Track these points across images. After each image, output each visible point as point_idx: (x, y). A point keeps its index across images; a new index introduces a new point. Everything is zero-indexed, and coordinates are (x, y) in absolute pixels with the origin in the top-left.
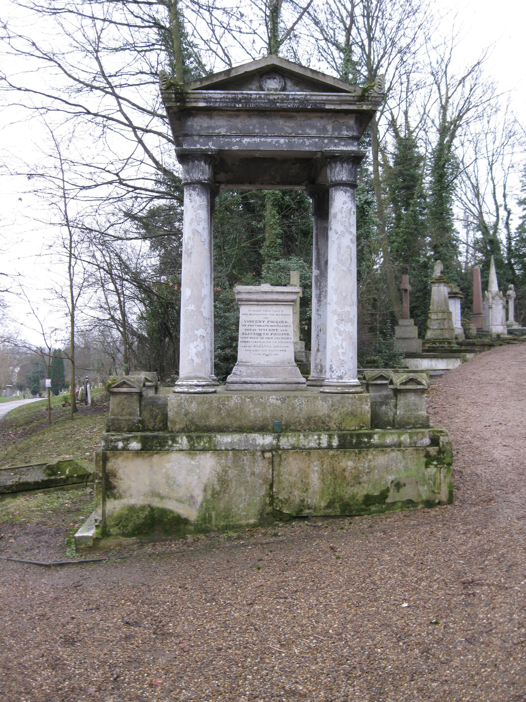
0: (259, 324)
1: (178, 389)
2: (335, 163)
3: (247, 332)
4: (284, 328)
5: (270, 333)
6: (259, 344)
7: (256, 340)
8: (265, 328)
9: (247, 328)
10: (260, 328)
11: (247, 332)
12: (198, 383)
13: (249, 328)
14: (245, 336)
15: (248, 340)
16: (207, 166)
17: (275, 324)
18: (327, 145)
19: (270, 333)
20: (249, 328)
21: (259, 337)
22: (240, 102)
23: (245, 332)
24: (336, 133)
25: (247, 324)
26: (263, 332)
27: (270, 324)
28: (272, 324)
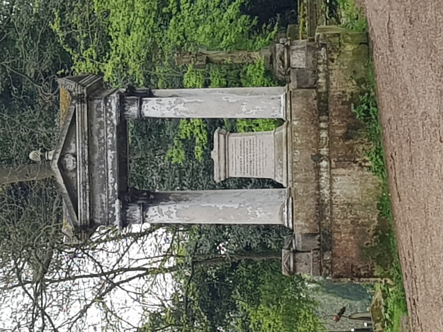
1: (291, 225)
2: (125, 115)
12: (286, 211)
16: (130, 207)
18: (112, 121)
24: (102, 115)
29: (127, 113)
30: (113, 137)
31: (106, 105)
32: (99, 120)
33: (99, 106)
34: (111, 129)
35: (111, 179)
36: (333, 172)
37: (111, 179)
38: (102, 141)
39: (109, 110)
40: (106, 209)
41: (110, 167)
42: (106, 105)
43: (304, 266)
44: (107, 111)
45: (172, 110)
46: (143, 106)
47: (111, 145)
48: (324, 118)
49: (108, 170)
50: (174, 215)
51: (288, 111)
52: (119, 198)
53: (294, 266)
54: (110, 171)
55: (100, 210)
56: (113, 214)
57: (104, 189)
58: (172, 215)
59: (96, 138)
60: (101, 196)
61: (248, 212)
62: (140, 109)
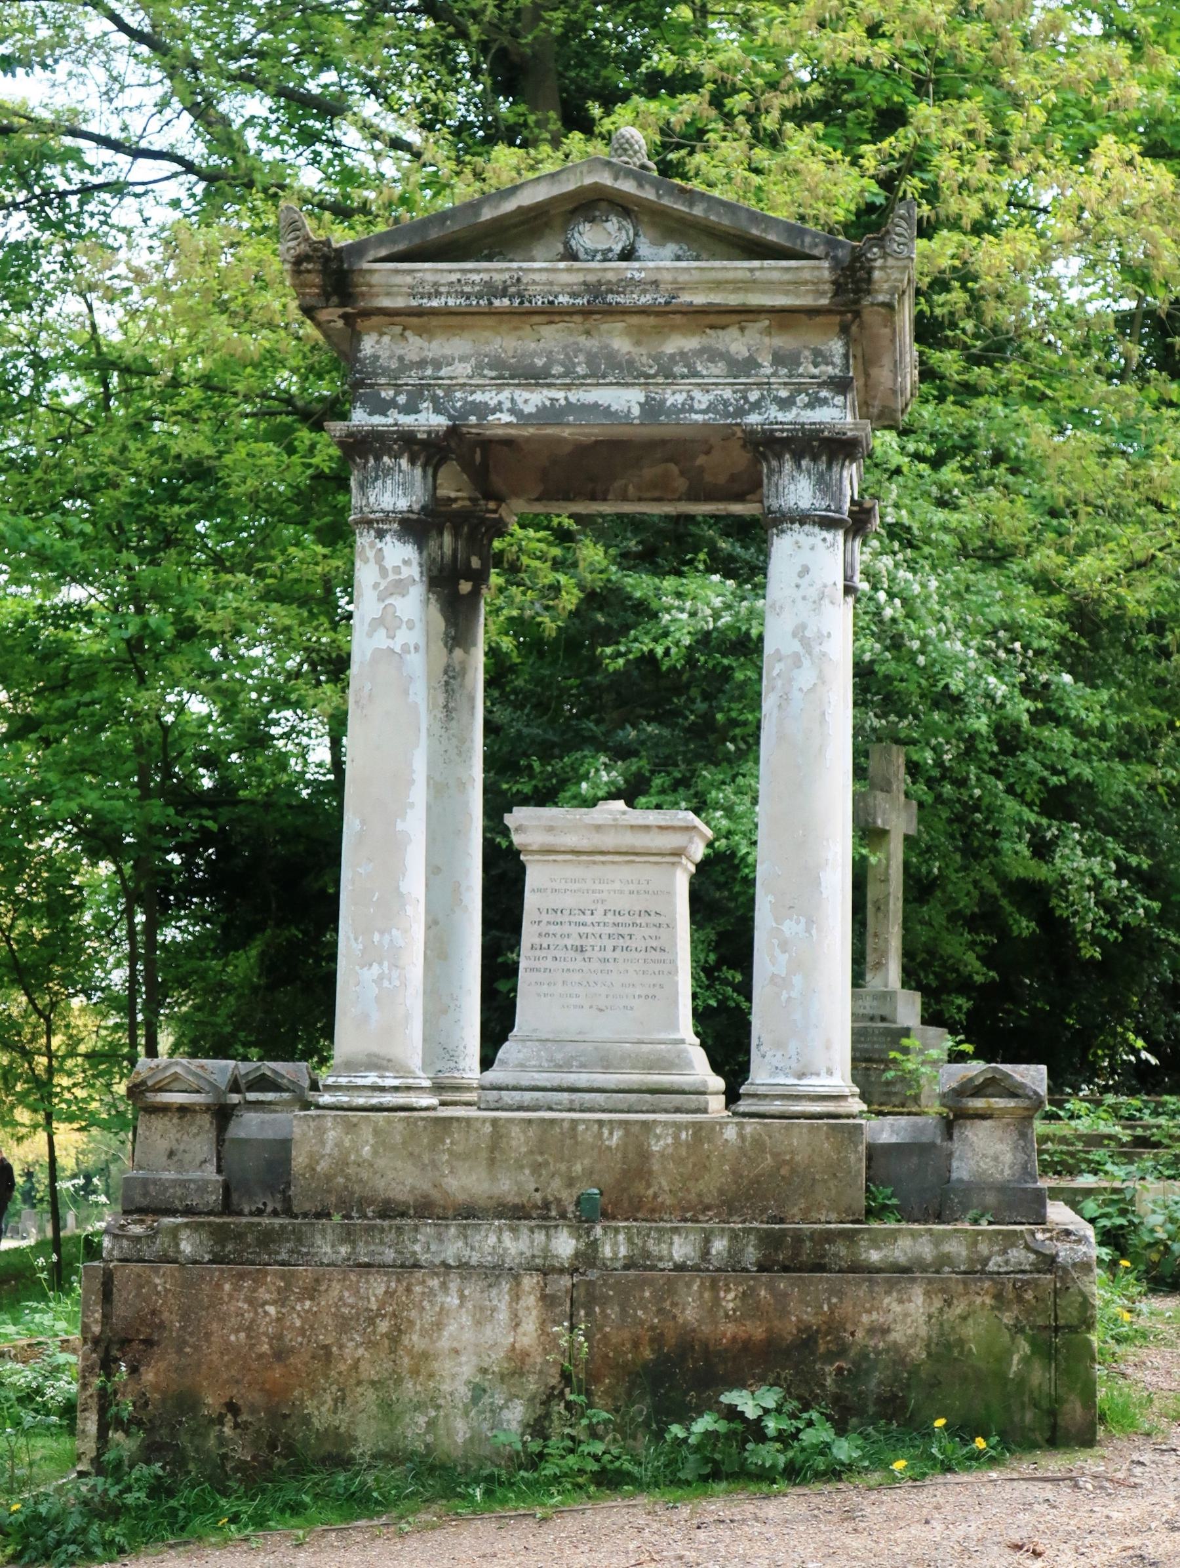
0: (582, 918)
2: (779, 457)
3: (545, 942)
4: (652, 931)
5: (610, 944)
6: (576, 977)
7: (571, 966)
8: (597, 930)
9: (544, 928)
10: (582, 930)
11: (545, 942)
12: (380, 1082)
13: (552, 929)
14: (538, 953)
15: (549, 963)
16: (418, 471)
17: (626, 919)
18: (756, 406)
19: (610, 944)
20: (552, 929)
21: (579, 956)
22: (504, 293)
23: (537, 941)
25: (545, 918)
26: (591, 941)
27: (610, 918)
28: (619, 919)
29: (788, 466)
30: (692, 410)
31: (820, 385)
32: (765, 361)
33: (820, 357)
34: (726, 403)
35: (532, 399)
36: (529, 1282)
37: (532, 399)
38: (679, 369)
39: (802, 399)
40: (411, 379)
41: (575, 396)
42: (820, 385)
43: (163, 1145)
44: (799, 389)
45: (796, 646)
46: (817, 530)
47: (664, 401)
48: (751, 1254)
49: (568, 387)
50: (381, 640)
51: (777, 1106)
52: (453, 431)
53: (164, 1109)
54: (560, 395)
55: (413, 356)
56: (392, 404)
57: (493, 374)
58: (382, 632)
59: (691, 343)
60: (462, 359)
61: (382, 933)
62: (803, 518)
